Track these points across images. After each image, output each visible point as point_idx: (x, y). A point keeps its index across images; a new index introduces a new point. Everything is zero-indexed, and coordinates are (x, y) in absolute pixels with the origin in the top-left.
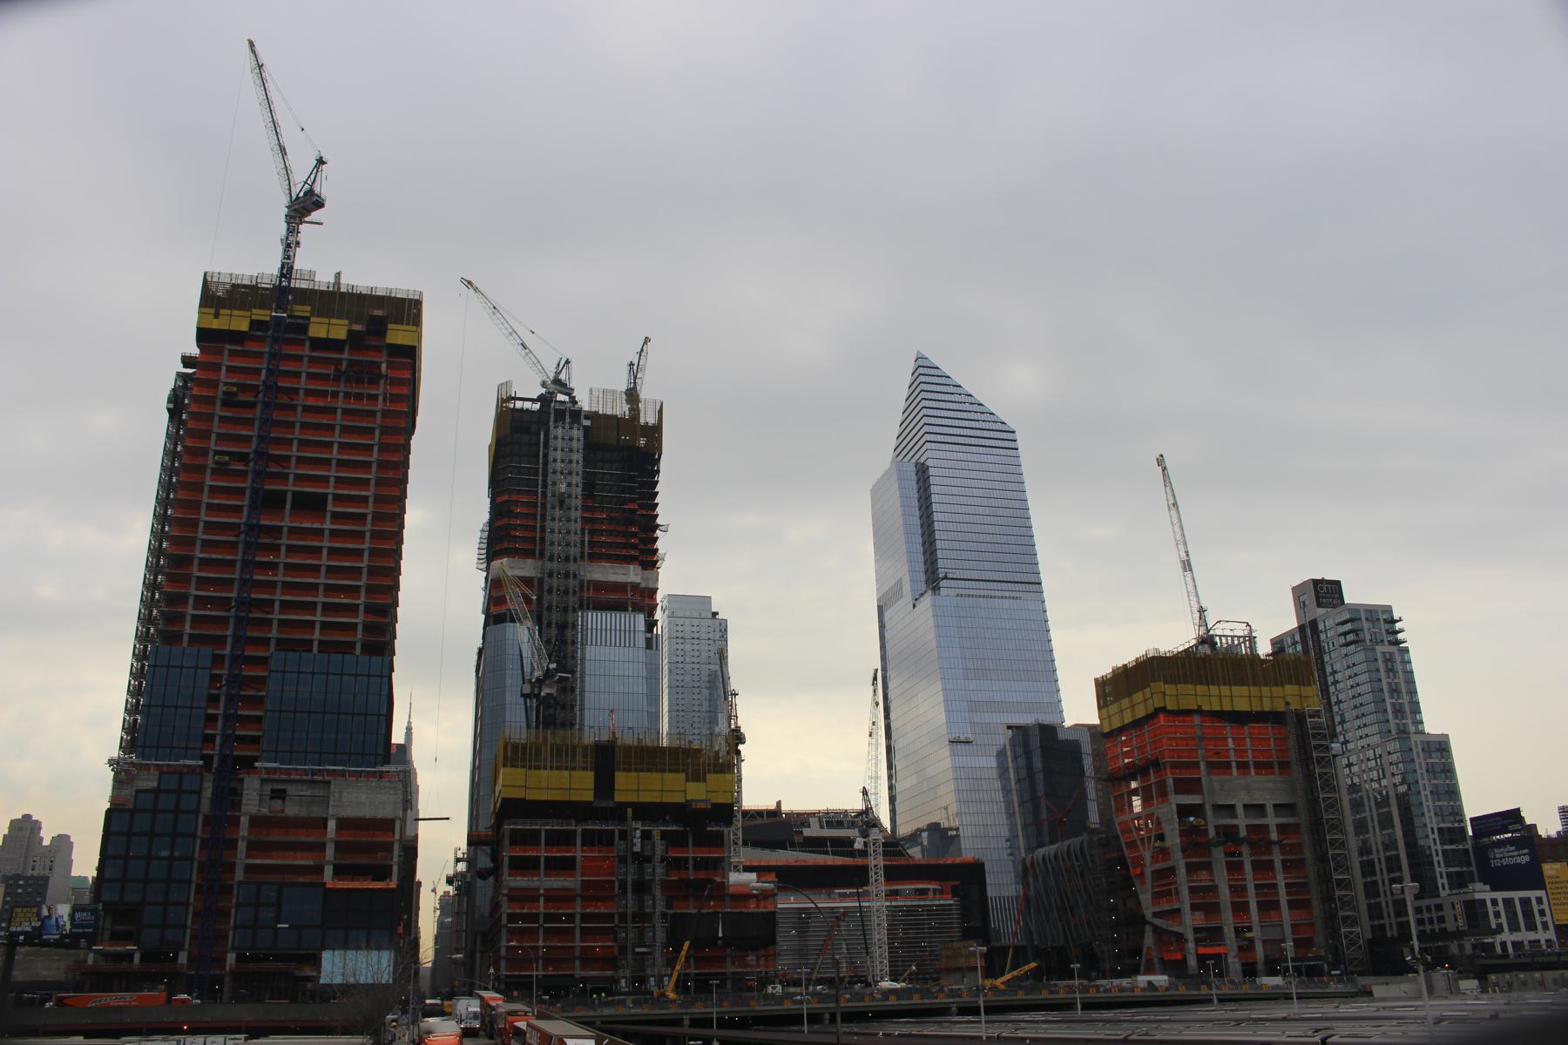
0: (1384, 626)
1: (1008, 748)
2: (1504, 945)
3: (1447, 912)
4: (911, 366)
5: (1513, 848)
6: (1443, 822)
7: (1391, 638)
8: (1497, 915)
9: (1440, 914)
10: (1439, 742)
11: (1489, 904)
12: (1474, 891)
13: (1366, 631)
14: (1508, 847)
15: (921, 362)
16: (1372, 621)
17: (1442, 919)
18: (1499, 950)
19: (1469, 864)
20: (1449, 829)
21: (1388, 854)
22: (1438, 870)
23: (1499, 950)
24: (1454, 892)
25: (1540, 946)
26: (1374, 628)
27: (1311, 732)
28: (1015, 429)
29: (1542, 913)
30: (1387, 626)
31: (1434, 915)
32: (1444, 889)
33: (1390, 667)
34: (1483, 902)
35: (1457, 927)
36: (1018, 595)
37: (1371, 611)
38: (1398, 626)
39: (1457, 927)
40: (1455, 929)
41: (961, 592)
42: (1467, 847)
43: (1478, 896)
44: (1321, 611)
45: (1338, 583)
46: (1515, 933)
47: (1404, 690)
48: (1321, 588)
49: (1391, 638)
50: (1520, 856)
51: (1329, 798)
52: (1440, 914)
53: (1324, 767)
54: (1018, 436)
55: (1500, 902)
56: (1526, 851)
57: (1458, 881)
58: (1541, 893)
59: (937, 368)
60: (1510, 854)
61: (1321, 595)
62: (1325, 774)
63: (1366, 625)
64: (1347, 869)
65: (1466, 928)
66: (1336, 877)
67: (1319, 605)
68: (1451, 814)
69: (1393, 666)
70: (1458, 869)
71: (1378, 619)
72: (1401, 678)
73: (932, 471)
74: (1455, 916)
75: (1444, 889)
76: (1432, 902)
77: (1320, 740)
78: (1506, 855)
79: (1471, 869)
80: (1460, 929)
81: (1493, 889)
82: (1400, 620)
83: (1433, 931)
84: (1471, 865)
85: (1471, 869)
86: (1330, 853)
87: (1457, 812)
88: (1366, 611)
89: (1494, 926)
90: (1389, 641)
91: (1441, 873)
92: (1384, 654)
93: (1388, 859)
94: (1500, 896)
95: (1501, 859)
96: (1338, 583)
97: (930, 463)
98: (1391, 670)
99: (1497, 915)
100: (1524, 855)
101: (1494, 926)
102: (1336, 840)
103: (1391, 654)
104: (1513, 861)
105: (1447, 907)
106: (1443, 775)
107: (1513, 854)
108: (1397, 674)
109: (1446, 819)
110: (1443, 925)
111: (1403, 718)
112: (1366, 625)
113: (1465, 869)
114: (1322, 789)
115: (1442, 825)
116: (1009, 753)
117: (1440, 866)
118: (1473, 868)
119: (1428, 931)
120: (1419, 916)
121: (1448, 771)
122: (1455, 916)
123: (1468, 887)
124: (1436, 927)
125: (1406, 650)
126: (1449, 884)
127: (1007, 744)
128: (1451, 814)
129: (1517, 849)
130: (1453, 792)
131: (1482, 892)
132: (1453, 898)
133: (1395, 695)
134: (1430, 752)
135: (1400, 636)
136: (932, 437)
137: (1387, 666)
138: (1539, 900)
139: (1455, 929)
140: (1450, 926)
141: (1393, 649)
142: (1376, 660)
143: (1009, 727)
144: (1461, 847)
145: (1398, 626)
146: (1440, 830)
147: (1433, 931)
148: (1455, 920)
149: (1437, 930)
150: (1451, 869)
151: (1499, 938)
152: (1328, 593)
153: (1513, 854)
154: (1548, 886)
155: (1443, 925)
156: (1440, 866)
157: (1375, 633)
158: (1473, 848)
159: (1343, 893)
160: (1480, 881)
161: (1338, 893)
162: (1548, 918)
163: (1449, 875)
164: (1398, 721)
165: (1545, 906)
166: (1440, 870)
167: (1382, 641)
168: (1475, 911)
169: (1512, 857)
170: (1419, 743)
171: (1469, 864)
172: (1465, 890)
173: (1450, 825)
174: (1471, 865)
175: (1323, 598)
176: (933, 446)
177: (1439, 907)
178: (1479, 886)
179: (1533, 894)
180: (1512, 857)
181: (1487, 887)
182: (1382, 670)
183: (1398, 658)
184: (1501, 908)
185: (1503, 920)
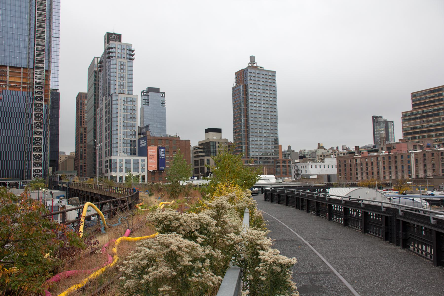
0: (126, 52)
2: (121, 178)
16: (121, 49)
48: (111, 36)
53: (39, 100)
58: (145, 158)
69: (124, 67)
72: (126, 72)
84: (136, 146)
85: (135, 148)
90: (127, 58)
92: (121, 62)
96: (120, 36)
98: (122, 69)
102: (38, 132)
103: (124, 62)
108: (125, 71)
111: (123, 88)
114: (35, 109)
121: (134, 110)
134: (127, 101)
137: (121, 67)
138: (143, 161)
142: (116, 64)
154: (148, 156)
159: (38, 153)
170: (122, 98)
174: (136, 146)
182: (117, 69)
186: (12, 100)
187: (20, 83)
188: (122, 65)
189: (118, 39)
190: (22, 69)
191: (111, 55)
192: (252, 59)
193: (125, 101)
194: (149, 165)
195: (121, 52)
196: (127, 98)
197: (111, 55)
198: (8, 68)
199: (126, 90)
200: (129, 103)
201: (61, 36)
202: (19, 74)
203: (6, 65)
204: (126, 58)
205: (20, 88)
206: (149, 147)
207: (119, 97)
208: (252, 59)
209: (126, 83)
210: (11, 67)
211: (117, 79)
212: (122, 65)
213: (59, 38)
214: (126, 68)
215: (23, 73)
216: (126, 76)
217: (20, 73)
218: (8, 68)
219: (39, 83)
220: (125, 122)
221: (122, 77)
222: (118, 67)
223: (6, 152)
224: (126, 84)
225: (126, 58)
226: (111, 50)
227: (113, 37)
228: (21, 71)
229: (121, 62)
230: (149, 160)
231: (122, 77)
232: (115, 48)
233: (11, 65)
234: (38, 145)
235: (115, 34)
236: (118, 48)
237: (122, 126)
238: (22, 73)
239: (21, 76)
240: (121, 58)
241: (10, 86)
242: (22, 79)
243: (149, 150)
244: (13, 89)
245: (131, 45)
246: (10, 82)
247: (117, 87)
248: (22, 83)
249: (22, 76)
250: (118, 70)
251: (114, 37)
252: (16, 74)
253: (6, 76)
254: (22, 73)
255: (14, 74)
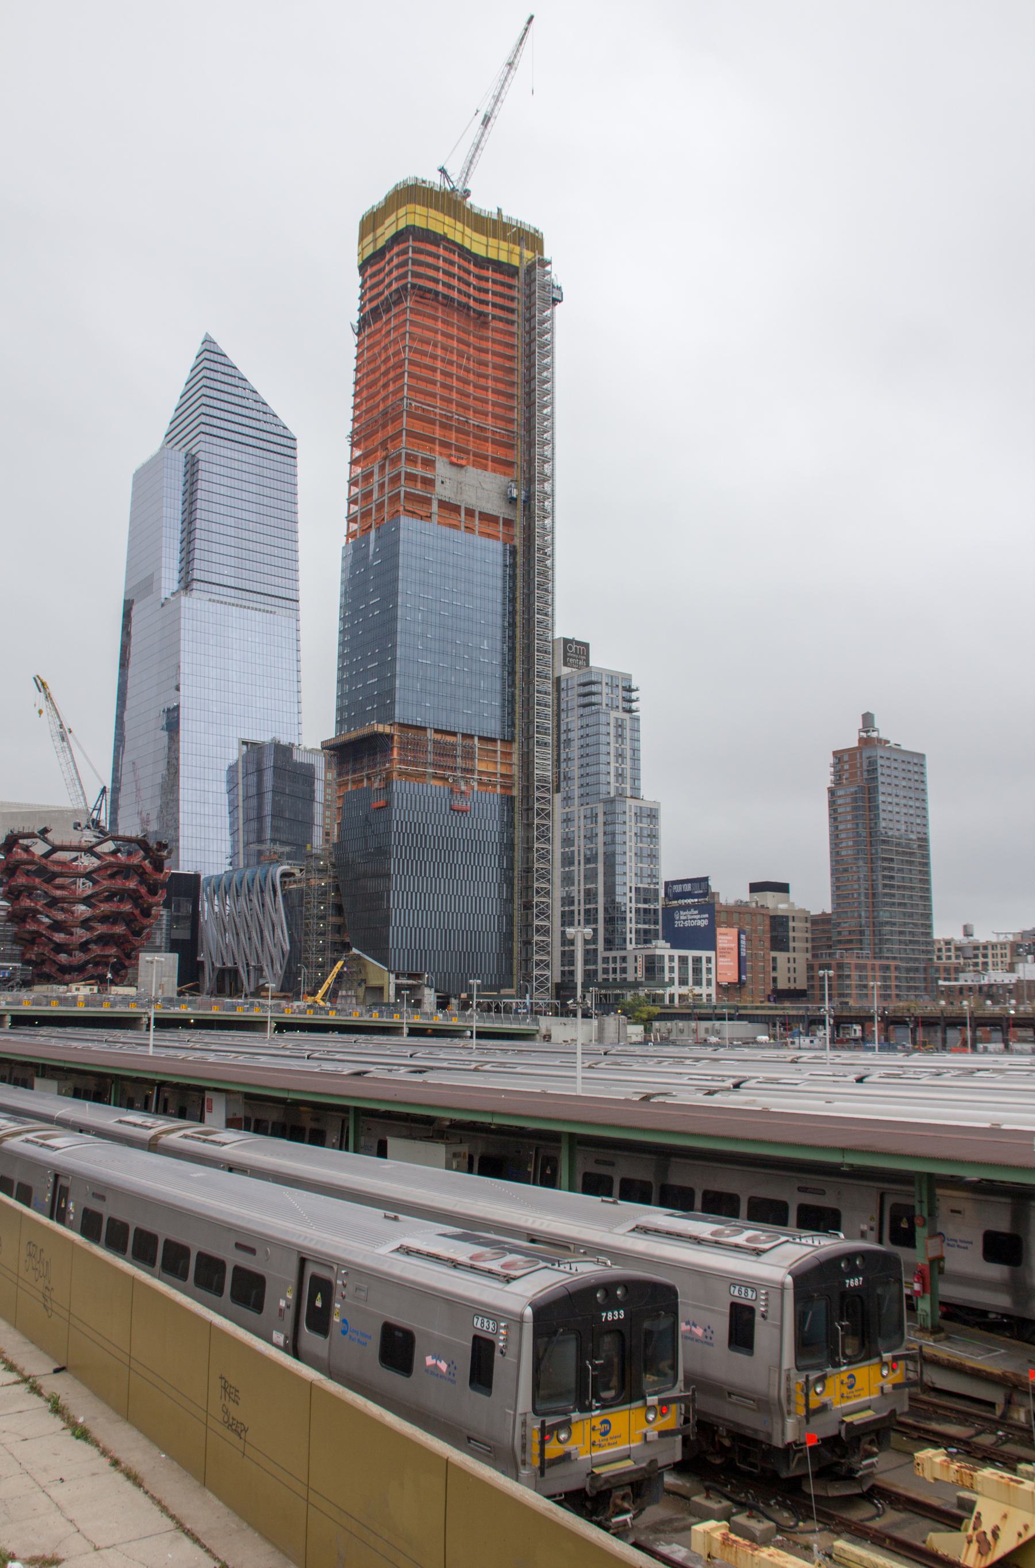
1: (240, 764)
2: (672, 996)
3: (630, 965)
4: (197, 348)
5: (696, 912)
6: (641, 883)
7: (626, 705)
8: (672, 969)
9: (624, 965)
10: (651, 809)
11: (666, 959)
12: (656, 947)
13: (604, 695)
14: (692, 910)
15: (207, 346)
16: (612, 686)
17: (624, 970)
18: (667, 1001)
19: (656, 923)
20: (645, 889)
21: (588, 906)
22: (628, 925)
23: (667, 1001)
24: (639, 946)
25: (701, 1000)
26: (612, 693)
27: (536, 784)
28: (296, 437)
29: (709, 970)
30: (625, 694)
31: (618, 966)
32: (631, 943)
33: (620, 733)
34: (662, 957)
35: (636, 978)
36: (273, 609)
37: (612, 677)
38: (634, 695)
39: (636, 978)
40: (634, 980)
41: (214, 597)
42: (657, 907)
43: (658, 952)
44: (565, 670)
45: (586, 646)
46: (683, 987)
47: (628, 757)
48: (571, 648)
49: (626, 705)
50: (700, 919)
51: (543, 849)
52: (624, 965)
53: (543, 818)
54: (299, 444)
55: (676, 959)
56: (707, 916)
57: (645, 937)
58: (711, 954)
59: (225, 356)
60: (693, 917)
61: (569, 654)
62: (543, 825)
63: (605, 690)
64: (548, 917)
65: (643, 979)
66: (536, 922)
67: (565, 664)
68: (649, 876)
69: (622, 731)
70: (646, 926)
71: (617, 686)
72: (627, 746)
73: (202, 465)
74: (636, 968)
75: (631, 943)
76: (618, 954)
77: (543, 792)
78: (689, 917)
79: (657, 927)
80: (638, 980)
81: (673, 947)
82: (637, 690)
83: (615, 979)
85: (657, 927)
86: (535, 900)
87: (653, 876)
88: (607, 676)
89: (667, 980)
90: (623, 708)
91: (631, 928)
92: (617, 719)
93: (587, 911)
94: (677, 953)
95: (684, 921)
96: (586, 646)
97: (201, 456)
99: (672, 969)
100: (704, 919)
101: (667, 980)
103: (622, 720)
104: (694, 923)
105: (630, 960)
106: (649, 840)
107: (695, 917)
109: (644, 879)
110: (624, 976)
111: (623, 783)
112: (605, 690)
113: (652, 927)
114: (538, 839)
115: (639, 885)
116: (240, 769)
117: (631, 923)
118: (659, 927)
119: (611, 980)
120: (605, 966)
122: (636, 968)
123: (651, 943)
124: (618, 976)
125: (638, 719)
126: (636, 939)
127: (241, 759)
128: (649, 876)
129: (699, 914)
130: (653, 856)
131: (662, 948)
132: (637, 952)
133: (620, 760)
134: (641, 817)
135: (634, 705)
136: (208, 429)
138: (709, 960)
139: (634, 980)
140: (630, 977)
141: (626, 716)
143: (245, 743)
144: (652, 907)
145: (634, 695)
146: (637, 889)
147: (615, 979)
148: (635, 972)
149: (618, 980)
150: (640, 926)
151: (669, 990)
152: (576, 653)
153: (695, 917)
154: (718, 950)
155: (624, 976)
156: (631, 923)
157: (612, 698)
158: (663, 909)
160: (663, 939)
161: (536, 938)
162: (713, 976)
163: (637, 931)
164: (618, 785)
165: (712, 965)
166: (631, 925)
167: (617, 707)
168: (652, 967)
169: (694, 919)
170: (633, 807)
171: (656, 923)
172: (648, 945)
173: (646, 886)
175: (570, 657)
176: (208, 438)
177: (624, 959)
178: (661, 943)
179: (704, 954)
180: (694, 919)
181: (668, 945)
183: (628, 724)
184: (676, 964)
185: (676, 975)
186: (485, 815)
187: (495, 774)
188: (620, 726)
189: (583, 655)
190: (499, 742)
191: (594, 699)
192: (868, 719)
193: (638, 816)
194: (719, 972)
195: (612, 693)
196: (641, 808)
197: (594, 699)
198: (476, 739)
199: (628, 786)
200: (644, 820)
201: (302, 596)
202: (493, 754)
203: (473, 733)
204: (620, 708)
205: (495, 786)
206: (719, 930)
207: (627, 806)
208: (868, 719)
209: (629, 770)
210: (481, 738)
211: (612, 759)
212: (620, 726)
213: (298, 601)
214: (628, 734)
215: (502, 752)
216: (628, 753)
217: (495, 752)
218: (476, 739)
219: (543, 779)
220: (639, 865)
221: (620, 756)
222: (612, 730)
223: (446, 930)
224: (628, 773)
225: (620, 708)
226: (594, 688)
227: (574, 649)
228: (496, 746)
229: (617, 719)
230: (720, 959)
231: (620, 756)
232: (600, 683)
233: (481, 735)
234: (542, 920)
235: (578, 643)
236: (607, 684)
237: (633, 875)
238: (499, 752)
239: (496, 757)
240: (612, 708)
241: (480, 783)
242: (499, 766)
243: (719, 938)
244: (485, 788)
245: (628, 678)
246: (480, 772)
247: (612, 779)
248: (499, 775)
249: (499, 760)
250: (612, 739)
251: (576, 648)
252: (489, 754)
253: (473, 759)
254: (499, 752)
255: (485, 754)
